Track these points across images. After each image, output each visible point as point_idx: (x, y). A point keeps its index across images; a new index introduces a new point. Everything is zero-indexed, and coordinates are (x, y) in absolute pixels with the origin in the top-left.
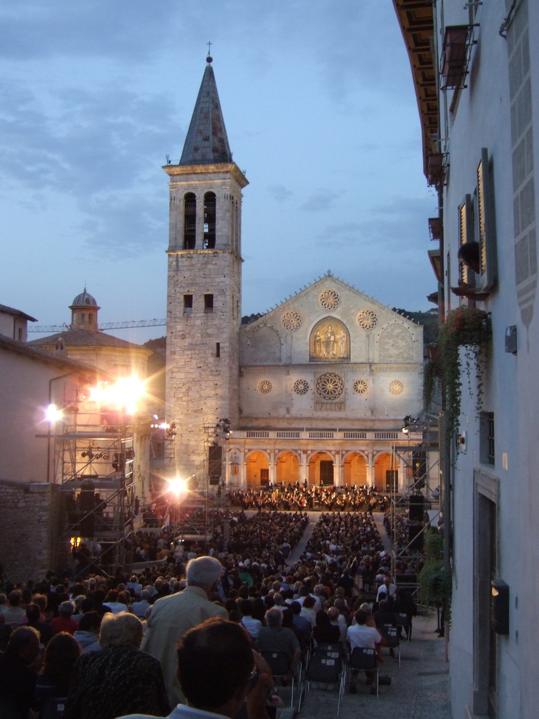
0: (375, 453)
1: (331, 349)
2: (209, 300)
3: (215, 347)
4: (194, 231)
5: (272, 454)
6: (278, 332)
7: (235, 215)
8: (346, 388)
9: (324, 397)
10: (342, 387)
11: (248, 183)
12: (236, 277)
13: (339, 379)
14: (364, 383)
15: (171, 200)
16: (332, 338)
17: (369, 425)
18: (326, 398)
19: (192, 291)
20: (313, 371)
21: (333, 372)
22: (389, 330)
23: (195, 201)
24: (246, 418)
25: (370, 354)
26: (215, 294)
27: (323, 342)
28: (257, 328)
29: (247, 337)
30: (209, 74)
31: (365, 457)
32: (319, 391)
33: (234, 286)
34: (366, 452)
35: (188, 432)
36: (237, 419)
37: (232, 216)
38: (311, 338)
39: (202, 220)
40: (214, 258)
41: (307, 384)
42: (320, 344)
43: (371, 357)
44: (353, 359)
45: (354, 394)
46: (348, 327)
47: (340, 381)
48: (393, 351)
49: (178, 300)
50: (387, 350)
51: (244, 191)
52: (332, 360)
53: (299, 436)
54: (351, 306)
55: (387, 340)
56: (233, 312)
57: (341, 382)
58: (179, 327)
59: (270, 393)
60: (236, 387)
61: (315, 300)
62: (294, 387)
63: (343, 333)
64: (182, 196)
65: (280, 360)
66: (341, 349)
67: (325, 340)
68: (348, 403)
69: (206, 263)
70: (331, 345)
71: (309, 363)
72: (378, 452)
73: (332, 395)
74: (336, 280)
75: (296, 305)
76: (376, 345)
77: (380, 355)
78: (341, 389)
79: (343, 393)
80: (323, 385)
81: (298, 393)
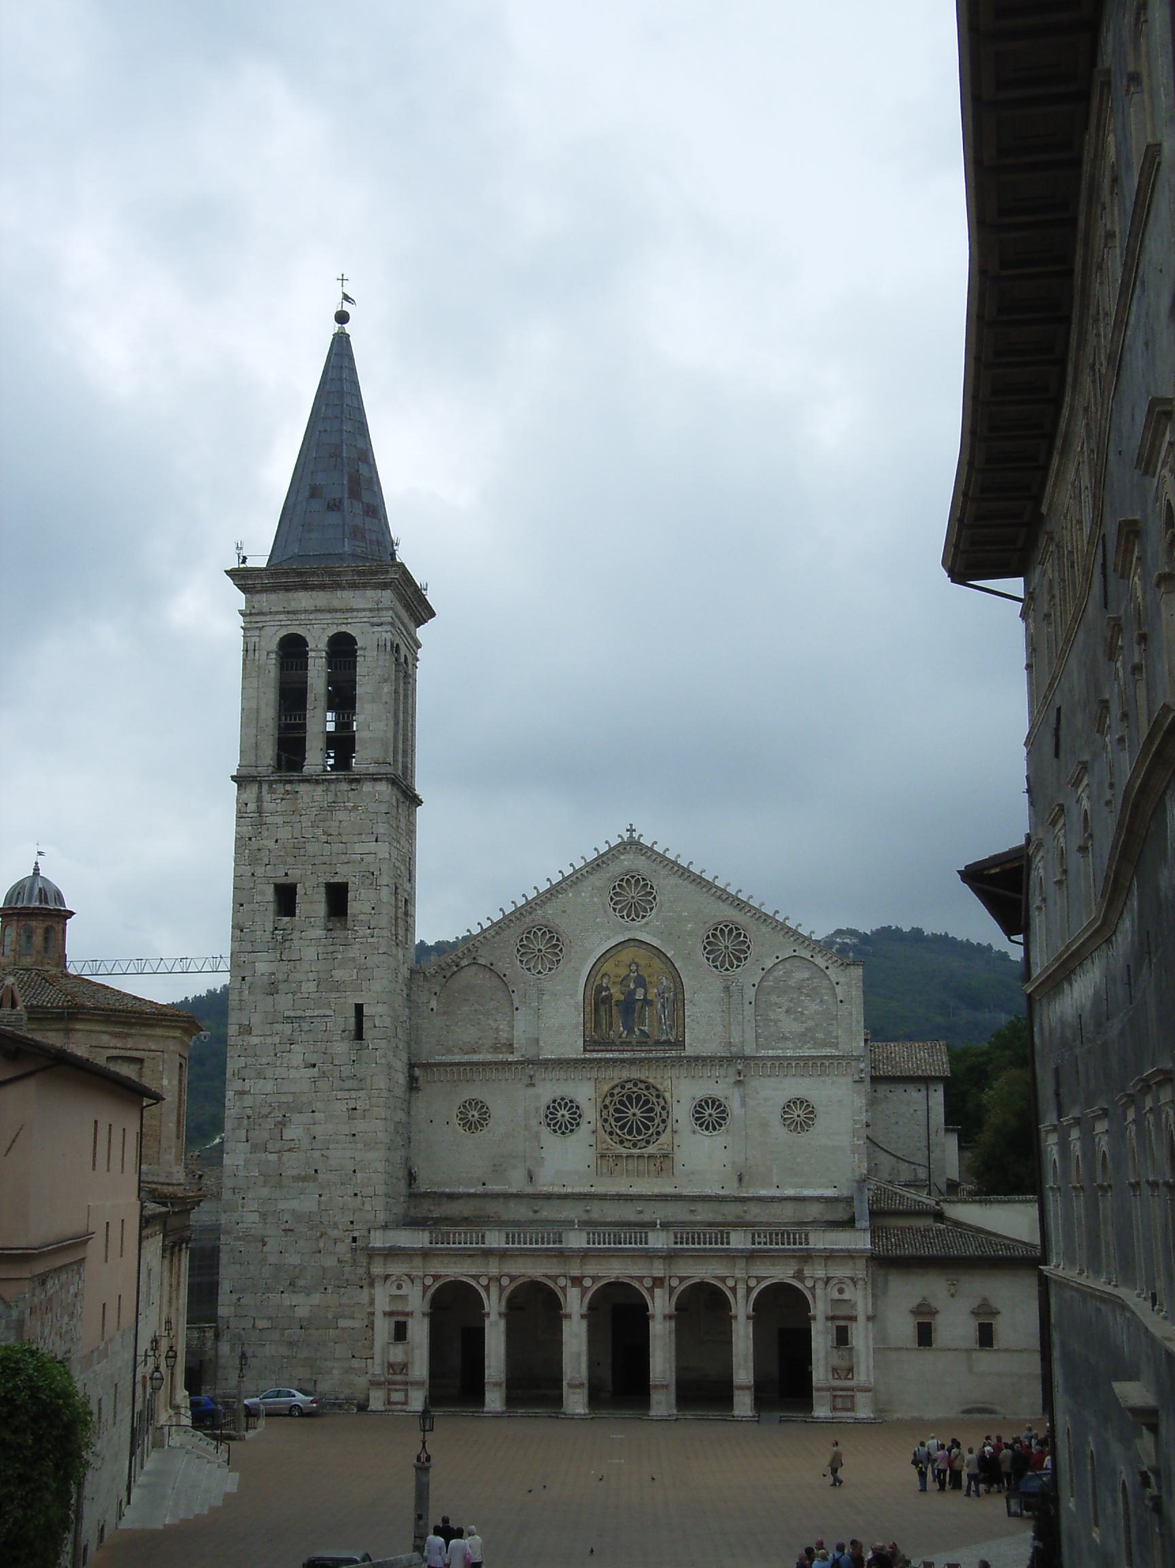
0: (752, 1283)
1: (636, 1020)
2: (337, 897)
3: (351, 1012)
4: (302, 727)
5: (494, 1290)
7: (401, 691)
9: (622, 1142)
11: (433, 614)
12: (403, 841)
13: (658, 1096)
14: (720, 1106)
15: (247, 651)
16: (639, 995)
17: (731, 1212)
19: (295, 875)
20: (594, 1074)
21: (643, 1078)
22: (779, 973)
23: (305, 655)
24: (426, 1195)
26: (353, 882)
28: (455, 969)
29: (429, 990)
30: (341, 350)
31: (729, 1294)
33: (398, 864)
34: (730, 1283)
35: (282, 1233)
36: (402, 1199)
37: (396, 692)
38: (588, 993)
39: (322, 702)
40: (351, 794)
41: (578, 1107)
43: (736, 1039)
44: (690, 1045)
47: (661, 1100)
48: (790, 1026)
49: (258, 898)
51: (422, 633)
52: (639, 1048)
53: (561, 1242)
55: (774, 998)
56: (396, 925)
57: (662, 1103)
58: (262, 967)
59: (486, 1129)
60: (401, 1116)
61: (595, 900)
62: (547, 1116)
63: (666, 978)
64: (274, 645)
65: (510, 1047)
66: (660, 1016)
67: (622, 997)
68: (680, 1156)
69: (332, 808)
70: (636, 1015)
71: (583, 1056)
72: (759, 1279)
73: (641, 1137)
74: (647, 852)
76: (749, 1010)
78: (664, 1121)
79: (669, 1129)
80: (617, 1110)
81: (555, 1131)
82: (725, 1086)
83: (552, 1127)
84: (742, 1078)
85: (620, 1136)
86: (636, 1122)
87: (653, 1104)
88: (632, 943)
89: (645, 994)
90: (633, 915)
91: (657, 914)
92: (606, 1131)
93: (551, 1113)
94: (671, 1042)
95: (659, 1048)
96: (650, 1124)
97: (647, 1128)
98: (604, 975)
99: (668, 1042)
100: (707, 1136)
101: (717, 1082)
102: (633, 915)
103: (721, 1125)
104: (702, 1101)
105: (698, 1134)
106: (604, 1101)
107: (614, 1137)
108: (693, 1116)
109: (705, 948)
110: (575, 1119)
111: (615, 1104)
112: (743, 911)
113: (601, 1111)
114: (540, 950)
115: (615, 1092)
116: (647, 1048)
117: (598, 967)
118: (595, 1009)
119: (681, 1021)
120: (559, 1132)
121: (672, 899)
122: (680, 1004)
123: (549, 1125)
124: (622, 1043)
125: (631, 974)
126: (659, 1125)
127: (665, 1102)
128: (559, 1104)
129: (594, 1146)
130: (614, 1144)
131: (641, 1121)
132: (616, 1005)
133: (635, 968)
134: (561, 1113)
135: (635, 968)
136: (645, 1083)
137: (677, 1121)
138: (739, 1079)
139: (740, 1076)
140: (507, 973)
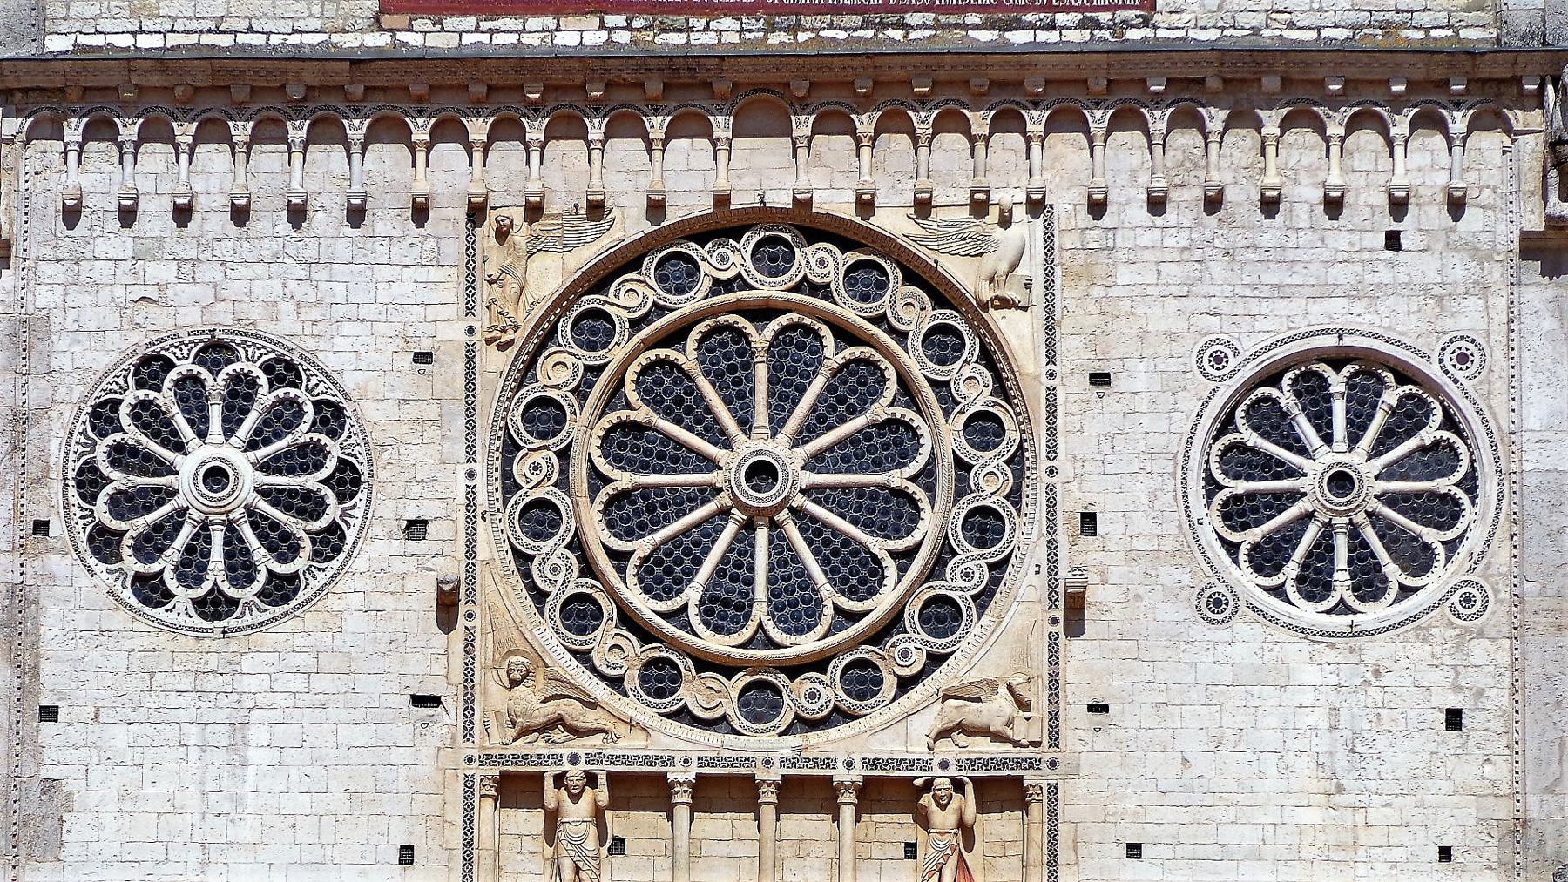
8: (1071, 503)
13: (942, 343)
18: (695, 692)
21: (835, 202)
32: (552, 554)
41: (331, 416)
45: (1217, 605)
57: (976, 393)
62: (89, 481)
73: (807, 644)
81: (151, 591)
82: (1459, 269)
83: (131, 564)
85: (645, 634)
92: (540, 597)
93: (123, 456)
96: (878, 546)
100: (1305, 632)
103: (1419, 559)
104: (1272, 377)
107: (606, 638)
108: (1212, 487)
110: (308, 505)
113: (511, 448)
120: (183, 595)
123: (104, 543)
126: (945, 552)
127: (1001, 388)
128: (191, 392)
130: (600, 691)
137: (1089, 522)
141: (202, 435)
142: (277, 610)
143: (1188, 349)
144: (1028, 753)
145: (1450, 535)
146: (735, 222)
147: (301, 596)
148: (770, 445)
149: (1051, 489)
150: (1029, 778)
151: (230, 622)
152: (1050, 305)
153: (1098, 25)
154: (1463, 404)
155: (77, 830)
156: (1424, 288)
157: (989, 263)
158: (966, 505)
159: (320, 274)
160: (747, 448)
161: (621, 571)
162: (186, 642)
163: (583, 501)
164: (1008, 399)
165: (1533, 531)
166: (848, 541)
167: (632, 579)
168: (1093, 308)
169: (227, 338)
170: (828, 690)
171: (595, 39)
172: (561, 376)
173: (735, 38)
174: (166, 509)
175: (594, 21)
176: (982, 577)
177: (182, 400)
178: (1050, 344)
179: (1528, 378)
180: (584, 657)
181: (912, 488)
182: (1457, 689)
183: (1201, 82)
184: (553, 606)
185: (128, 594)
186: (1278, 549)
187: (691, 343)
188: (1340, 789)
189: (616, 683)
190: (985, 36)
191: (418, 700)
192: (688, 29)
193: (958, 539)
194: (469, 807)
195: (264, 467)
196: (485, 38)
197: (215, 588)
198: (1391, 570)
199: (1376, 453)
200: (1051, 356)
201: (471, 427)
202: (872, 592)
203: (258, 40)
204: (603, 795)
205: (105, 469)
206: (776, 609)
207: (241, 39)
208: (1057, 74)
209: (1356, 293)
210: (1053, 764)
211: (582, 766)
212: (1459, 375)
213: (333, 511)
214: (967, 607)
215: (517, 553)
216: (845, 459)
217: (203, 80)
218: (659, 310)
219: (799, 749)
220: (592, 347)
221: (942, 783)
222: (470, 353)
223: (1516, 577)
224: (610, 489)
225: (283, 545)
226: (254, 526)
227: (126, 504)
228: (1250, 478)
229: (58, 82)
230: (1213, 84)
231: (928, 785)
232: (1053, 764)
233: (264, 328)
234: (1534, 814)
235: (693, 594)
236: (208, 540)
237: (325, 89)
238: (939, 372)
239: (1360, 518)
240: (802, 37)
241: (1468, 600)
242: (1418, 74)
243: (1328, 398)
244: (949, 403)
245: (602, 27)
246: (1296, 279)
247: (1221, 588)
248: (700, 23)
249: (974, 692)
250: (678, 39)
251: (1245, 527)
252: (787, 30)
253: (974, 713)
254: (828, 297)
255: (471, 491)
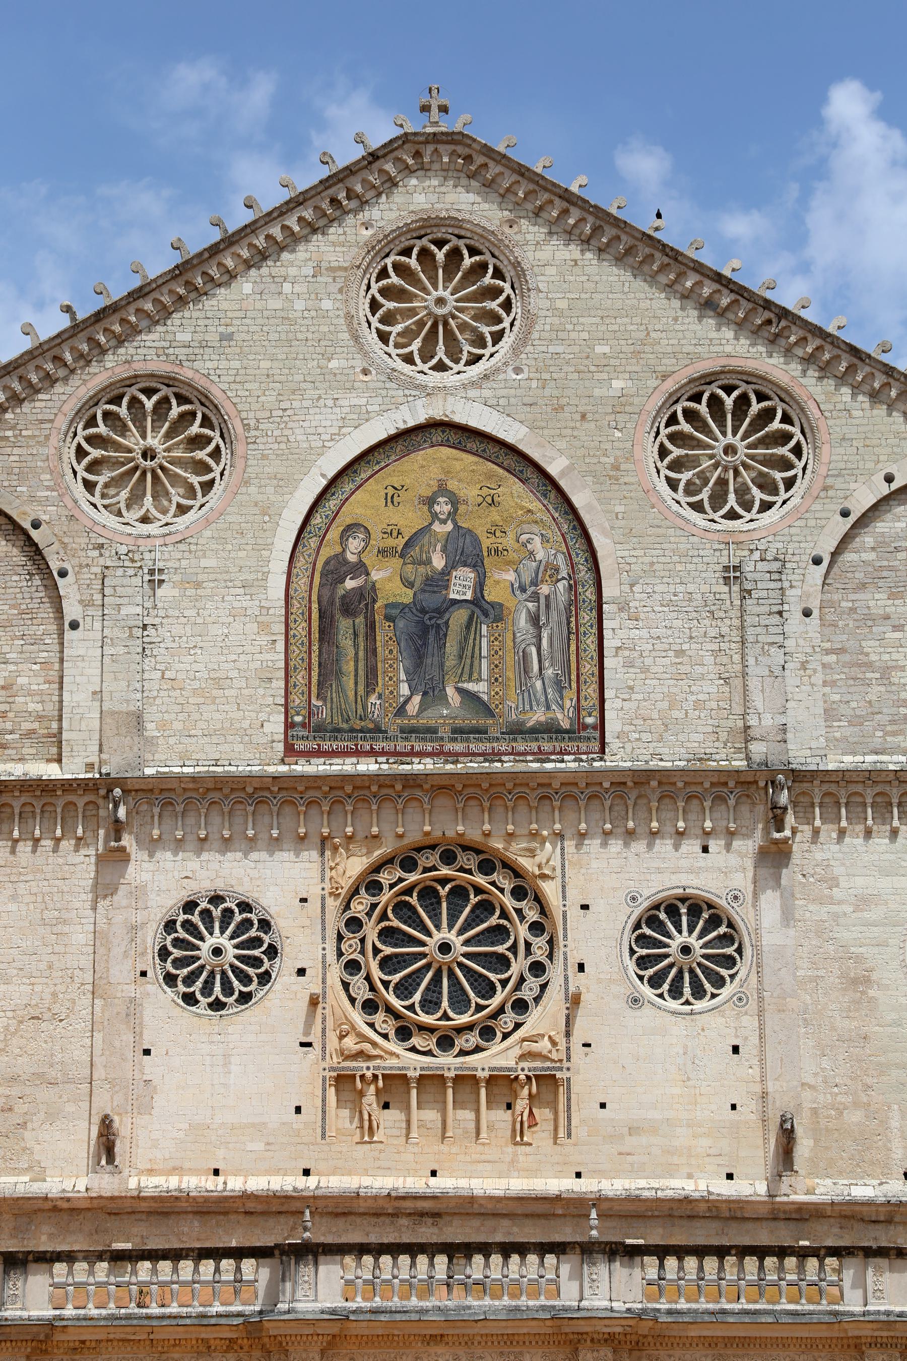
1: (450, 662)
6: (34, 534)
9: (404, 1033)
10: (540, 954)
21: (474, 835)
25: (757, 700)
27: (395, 611)
42: (371, 626)
46: (577, 500)
50: (886, 672)
52: (458, 747)
54: (606, 349)
61: (327, 304)
62: (164, 953)
66: (525, 655)
67: (407, 596)
71: (283, 769)
73: (464, 1019)
75: (184, 337)
77: (830, 714)
78: (537, 968)
79: (555, 995)
80: (387, 935)
83: (182, 988)
84: (787, 833)
85: (397, 1016)
86: (451, 974)
87: (504, 915)
88: (437, 436)
89: (480, 585)
90: (441, 353)
91: (516, 350)
92: (352, 1000)
93: (177, 942)
94: (560, 731)
95: (521, 747)
96: (493, 977)
97: (488, 990)
98: (350, 529)
99: (550, 729)
100: (673, 1013)
101: (705, 850)
102: (441, 353)
103: (719, 982)
104: (657, 907)
105: (647, 1010)
106: (347, 907)
108: (632, 952)
109: (663, 452)
111: (384, 917)
112: (782, 342)
113: (340, 938)
114: (149, 454)
115: (385, 878)
116: (482, 747)
117: (332, 504)
118: (322, 631)
119: (589, 668)
120: (204, 1001)
121: (562, 304)
122: (587, 617)
123: (170, 979)
124: (409, 731)
125: (437, 527)
126: (522, 980)
127: (543, 912)
128: (206, 915)
129: (317, 1045)
131: (461, 965)
132: (388, 618)
133: (447, 508)
134: (211, 941)
135: (447, 508)
136: (478, 852)
137: (581, 967)
138: (777, 835)
139: (780, 829)
140: (44, 517)
141: (211, 934)
142: (243, 1007)
143: (621, 894)
144: (558, 1065)
145: (732, 972)
146: (432, 842)
147: (253, 1001)
148: (448, 935)
149: (565, 954)
150: (559, 1075)
151: (223, 1012)
152: (564, 876)
153: (582, 761)
154: (736, 917)
155: (159, 1101)
156: (719, 869)
157: (538, 859)
158: (531, 960)
159: (260, 866)
160: (438, 937)
161: (387, 989)
162: (205, 1021)
163: (371, 959)
164: (546, 916)
165: (766, 970)
166: (481, 975)
167: (391, 992)
168: (582, 878)
169: (221, 893)
170: (473, 1039)
171: (374, 767)
172: (360, 908)
173: (432, 767)
174: (196, 965)
175: (373, 759)
176: (536, 991)
177: (203, 920)
178: (564, 892)
179: (763, 906)
180: (372, 1025)
181: (507, 953)
182: (737, 1036)
183: (625, 783)
184: (359, 1004)
185: (180, 1002)
186: (660, 978)
187: (415, 894)
188: (689, 1079)
189: (385, 1036)
190: (535, 765)
191: (303, 1045)
192: (412, 763)
193: (527, 975)
194: (324, 1090)
195: (237, 947)
196: (328, 767)
197: (217, 998)
198: (707, 986)
199: (700, 937)
200: (564, 898)
201: (324, 929)
202: (491, 997)
203: (233, 769)
204: (381, 1083)
205: (170, 948)
206: (451, 1004)
207: (227, 768)
208: (565, 781)
209: (690, 871)
210: (568, 1069)
211: (371, 1071)
212: (735, 905)
213: (267, 964)
214: (531, 1003)
215: (342, 981)
216: (479, 941)
217: (211, 785)
218: (401, 880)
219: (462, 1063)
220: (374, 895)
221: (522, 1077)
222: (323, 898)
223: (759, 991)
224: (381, 955)
225: (246, 979)
226: (233, 972)
227: (179, 963)
228: (647, 948)
229: (150, 787)
230: (630, 784)
231: (517, 1078)
232: (568, 1069)
233: (236, 889)
234: (770, 1090)
235: (417, 997)
236: (214, 978)
237: (261, 789)
238: (518, 905)
239: (695, 965)
240: (459, 766)
241: (740, 999)
242: (715, 780)
243: (680, 915)
244: (522, 917)
245: (376, 762)
246: (666, 865)
247: (636, 994)
248: (416, 760)
249: (535, 1039)
250: (408, 767)
251: (646, 969)
252: (452, 763)
253: (535, 1047)
254: (471, 874)
255: (324, 956)
